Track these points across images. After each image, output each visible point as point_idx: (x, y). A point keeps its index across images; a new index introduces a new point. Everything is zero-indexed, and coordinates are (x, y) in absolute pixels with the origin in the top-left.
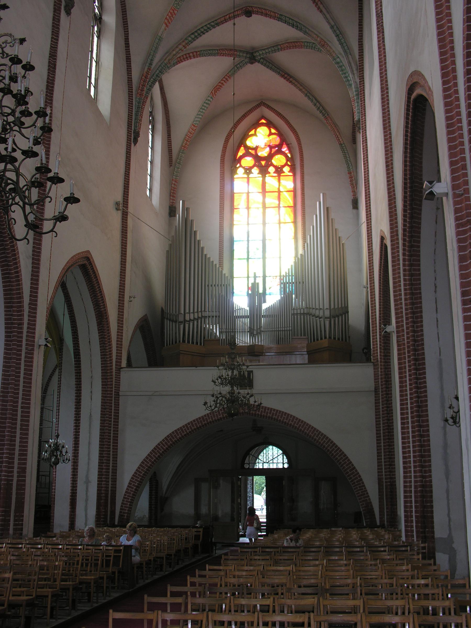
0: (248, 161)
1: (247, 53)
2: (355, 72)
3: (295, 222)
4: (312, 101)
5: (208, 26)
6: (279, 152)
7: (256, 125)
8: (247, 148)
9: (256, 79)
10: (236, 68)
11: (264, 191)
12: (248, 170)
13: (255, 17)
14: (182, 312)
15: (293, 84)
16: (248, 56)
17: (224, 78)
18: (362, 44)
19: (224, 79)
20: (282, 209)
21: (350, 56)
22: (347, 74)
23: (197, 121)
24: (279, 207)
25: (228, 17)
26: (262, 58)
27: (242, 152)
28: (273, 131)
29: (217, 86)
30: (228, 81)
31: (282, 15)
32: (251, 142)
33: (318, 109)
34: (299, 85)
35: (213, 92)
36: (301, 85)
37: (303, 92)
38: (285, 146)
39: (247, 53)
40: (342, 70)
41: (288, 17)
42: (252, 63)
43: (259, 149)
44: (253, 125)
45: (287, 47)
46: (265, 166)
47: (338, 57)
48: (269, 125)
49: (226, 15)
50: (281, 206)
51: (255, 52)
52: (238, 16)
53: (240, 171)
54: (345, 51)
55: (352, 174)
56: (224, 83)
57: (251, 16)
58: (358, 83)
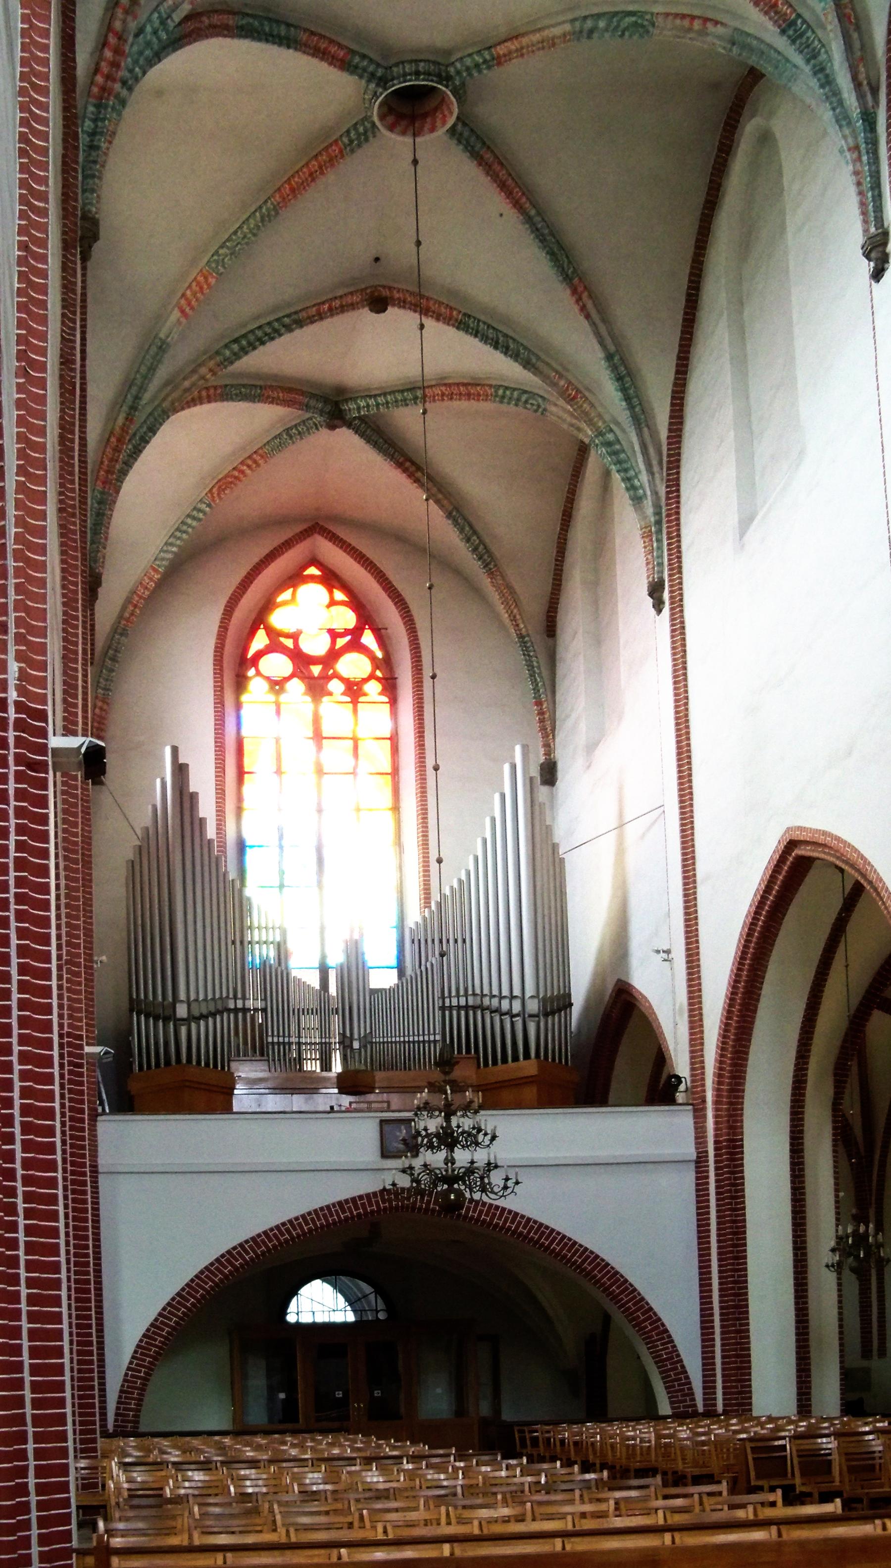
1: (326, 400)
2: (656, 469)
5: (276, 325)
6: (355, 645)
7: (295, 579)
8: (272, 633)
10: (289, 435)
13: (392, 312)
16: (328, 408)
17: (250, 457)
19: (249, 462)
21: (645, 430)
22: (632, 473)
25: (326, 306)
26: (360, 418)
27: (260, 640)
28: (339, 595)
29: (226, 476)
30: (258, 465)
31: (469, 316)
33: (475, 550)
35: (215, 490)
36: (440, 491)
39: (326, 400)
40: (619, 462)
41: (484, 323)
42: (332, 427)
45: (443, 395)
47: (611, 430)
49: (323, 303)
51: (346, 401)
52: (353, 306)
56: (248, 472)
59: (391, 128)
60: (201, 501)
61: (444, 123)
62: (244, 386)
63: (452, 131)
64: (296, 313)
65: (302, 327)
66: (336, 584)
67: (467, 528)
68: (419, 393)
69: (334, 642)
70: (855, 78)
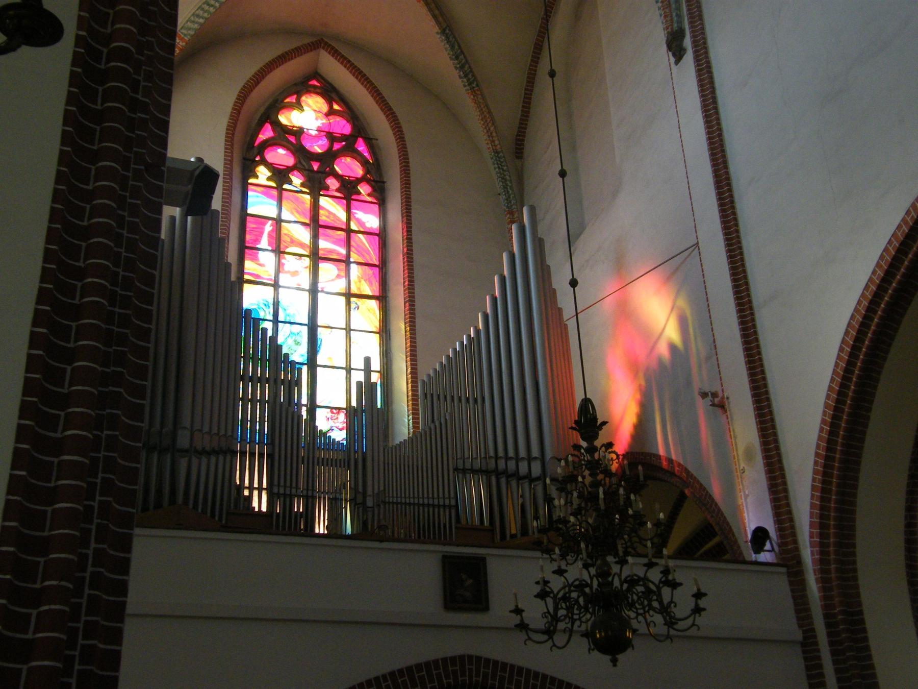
3: (382, 298)
11: (316, 224)
12: (280, 175)
20: (354, 267)
28: (336, 107)
32: (290, 118)
38: (360, 140)
44: (295, 84)
46: (317, 172)
48: (329, 92)
50: (352, 260)
53: (263, 174)
66: (336, 98)
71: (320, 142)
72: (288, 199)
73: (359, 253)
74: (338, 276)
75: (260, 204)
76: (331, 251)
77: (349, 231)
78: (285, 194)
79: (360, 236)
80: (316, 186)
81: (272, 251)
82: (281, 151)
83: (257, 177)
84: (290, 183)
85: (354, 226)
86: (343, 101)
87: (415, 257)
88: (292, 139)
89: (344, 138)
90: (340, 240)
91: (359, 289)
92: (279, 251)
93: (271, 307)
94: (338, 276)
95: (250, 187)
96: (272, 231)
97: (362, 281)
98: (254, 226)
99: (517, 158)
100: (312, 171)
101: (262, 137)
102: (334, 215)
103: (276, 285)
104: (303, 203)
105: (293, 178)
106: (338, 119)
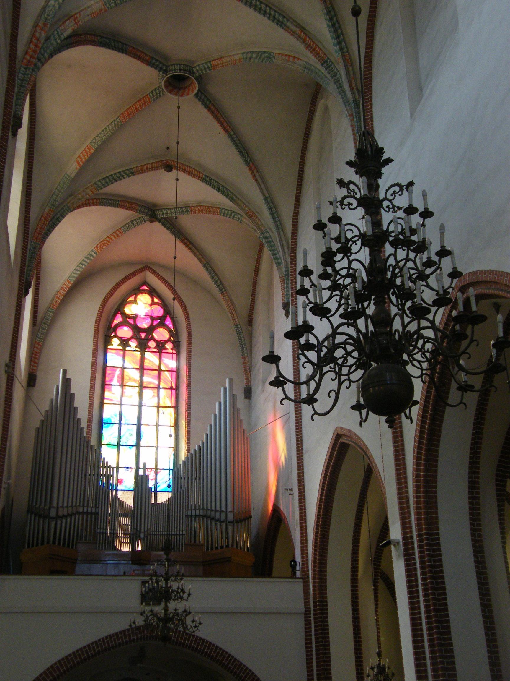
0: (125, 332)
1: (149, 209)
3: (176, 407)
4: (210, 273)
7: (137, 291)
9: (156, 242)
10: (133, 224)
11: (142, 369)
12: (125, 342)
14: (55, 505)
15: (192, 251)
16: (150, 213)
17: (115, 232)
18: (297, 222)
19: (115, 234)
22: (276, 252)
23: (73, 277)
24: (158, 388)
26: (164, 218)
28: (156, 300)
29: (104, 240)
30: (119, 236)
31: (207, 177)
32: (130, 310)
34: (198, 254)
35: (98, 246)
37: (201, 262)
39: (149, 209)
41: (214, 180)
42: (152, 222)
43: (138, 318)
44: (134, 290)
45: (199, 210)
47: (267, 232)
48: (152, 292)
50: (161, 387)
51: (158, 210)
53: (115, 342)
54: (277, 227)
55: (247, 359)
56: (114, 239)
57: (171, 171)
58: (289, 263)
59: (170, 92)
60: (92, 251)
61: (193, 92)
62: (111, 200)
63: (196, 95)
64: (132, 169)
65: (134, 175)
66: (155, 295)
67: (212, 273)
68: (189, 209)
69: (152, 322)
70: (350, 85)
71: (147, 321)
72: (128, 355)
73: (165, 383)
74: (154, 396)
75: (113, 359)
76: (150, 383)
77: (160, 371)
78: (127, 352)
79: (166, 372)
80: (143, 347)
81: (119, 385)
82: (126, 329)
83: (112, 345)
84: (130, 346)
85: (163, 368)
86: (159, 297)
87: (192, 385)
88: (131, 321)
89: (159, 318)
90: (155, 376)
91: (164, 403)
92: (122, 385)
93: (118, 416)
94: (154, 396)
95: (109, 351)
96: (120, 374)
97: (166, 397)
98: (110, 372)
99: (249, 325)
100: (141, 339)
101: (116, 322)
102: (152, 362)
103: (121, 404)
104: (136, 357)
105: (130, 343)
106: (157, 306)
